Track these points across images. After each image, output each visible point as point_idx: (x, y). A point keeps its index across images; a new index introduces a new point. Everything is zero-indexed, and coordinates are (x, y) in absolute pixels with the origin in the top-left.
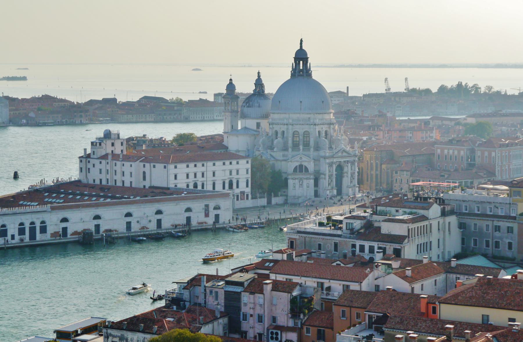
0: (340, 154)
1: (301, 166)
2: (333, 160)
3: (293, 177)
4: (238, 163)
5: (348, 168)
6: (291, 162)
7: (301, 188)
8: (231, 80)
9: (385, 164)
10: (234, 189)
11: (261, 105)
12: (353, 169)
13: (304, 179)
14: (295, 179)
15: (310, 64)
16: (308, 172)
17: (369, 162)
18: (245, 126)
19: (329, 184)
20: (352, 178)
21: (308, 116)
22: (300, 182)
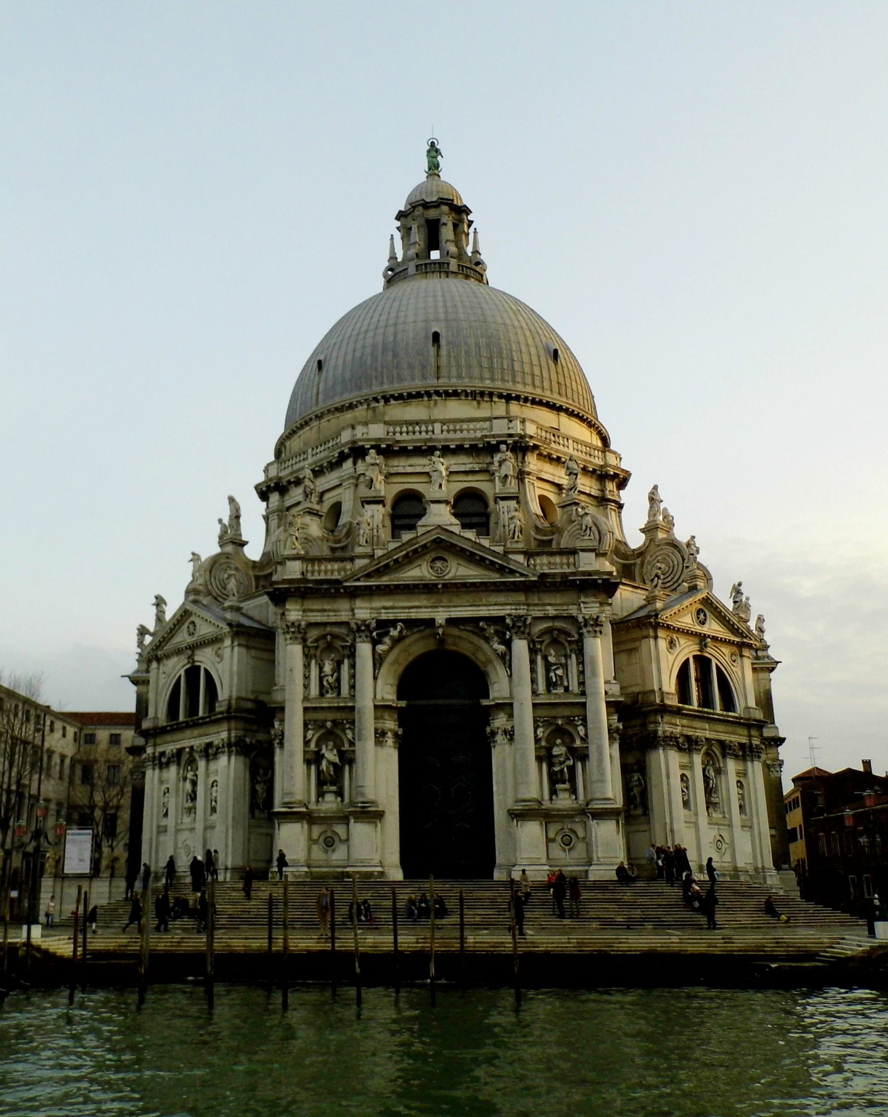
5: (510, 676)
7: (187, 820)
20: (559, 750)
22: (185, 779)
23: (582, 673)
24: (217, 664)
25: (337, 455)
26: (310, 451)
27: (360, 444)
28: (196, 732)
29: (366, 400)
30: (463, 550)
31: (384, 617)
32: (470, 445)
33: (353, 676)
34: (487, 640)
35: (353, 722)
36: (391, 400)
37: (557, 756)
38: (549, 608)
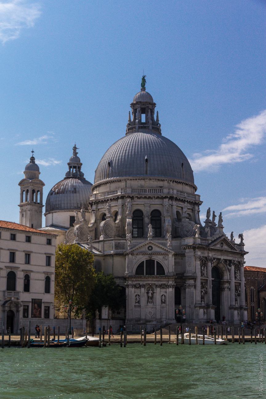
0: (218, 246)
1: (150, 263)
2: (208, 253)
3: (135, 283)
4: (28, 240)
5: (230, 275)
6: (132, 254)
7: (150, 305)
10: (18, 292)
11: (77, 190)
12: (238, 277)
13: (157, 286)
14: (140, 286)
15: (157, 113)
18: (51, 223)
19: (201, 298)
20: (236, 294)
21: (160, 184)
22: (148, 293)
23: (240, 275)
24: (164, 261)
26: (147, 190)
28: (154, 280)
30: (228, 242)
31: (215, 257)
34: (226, 265)
35: (207, 284)
36: (174, 182)
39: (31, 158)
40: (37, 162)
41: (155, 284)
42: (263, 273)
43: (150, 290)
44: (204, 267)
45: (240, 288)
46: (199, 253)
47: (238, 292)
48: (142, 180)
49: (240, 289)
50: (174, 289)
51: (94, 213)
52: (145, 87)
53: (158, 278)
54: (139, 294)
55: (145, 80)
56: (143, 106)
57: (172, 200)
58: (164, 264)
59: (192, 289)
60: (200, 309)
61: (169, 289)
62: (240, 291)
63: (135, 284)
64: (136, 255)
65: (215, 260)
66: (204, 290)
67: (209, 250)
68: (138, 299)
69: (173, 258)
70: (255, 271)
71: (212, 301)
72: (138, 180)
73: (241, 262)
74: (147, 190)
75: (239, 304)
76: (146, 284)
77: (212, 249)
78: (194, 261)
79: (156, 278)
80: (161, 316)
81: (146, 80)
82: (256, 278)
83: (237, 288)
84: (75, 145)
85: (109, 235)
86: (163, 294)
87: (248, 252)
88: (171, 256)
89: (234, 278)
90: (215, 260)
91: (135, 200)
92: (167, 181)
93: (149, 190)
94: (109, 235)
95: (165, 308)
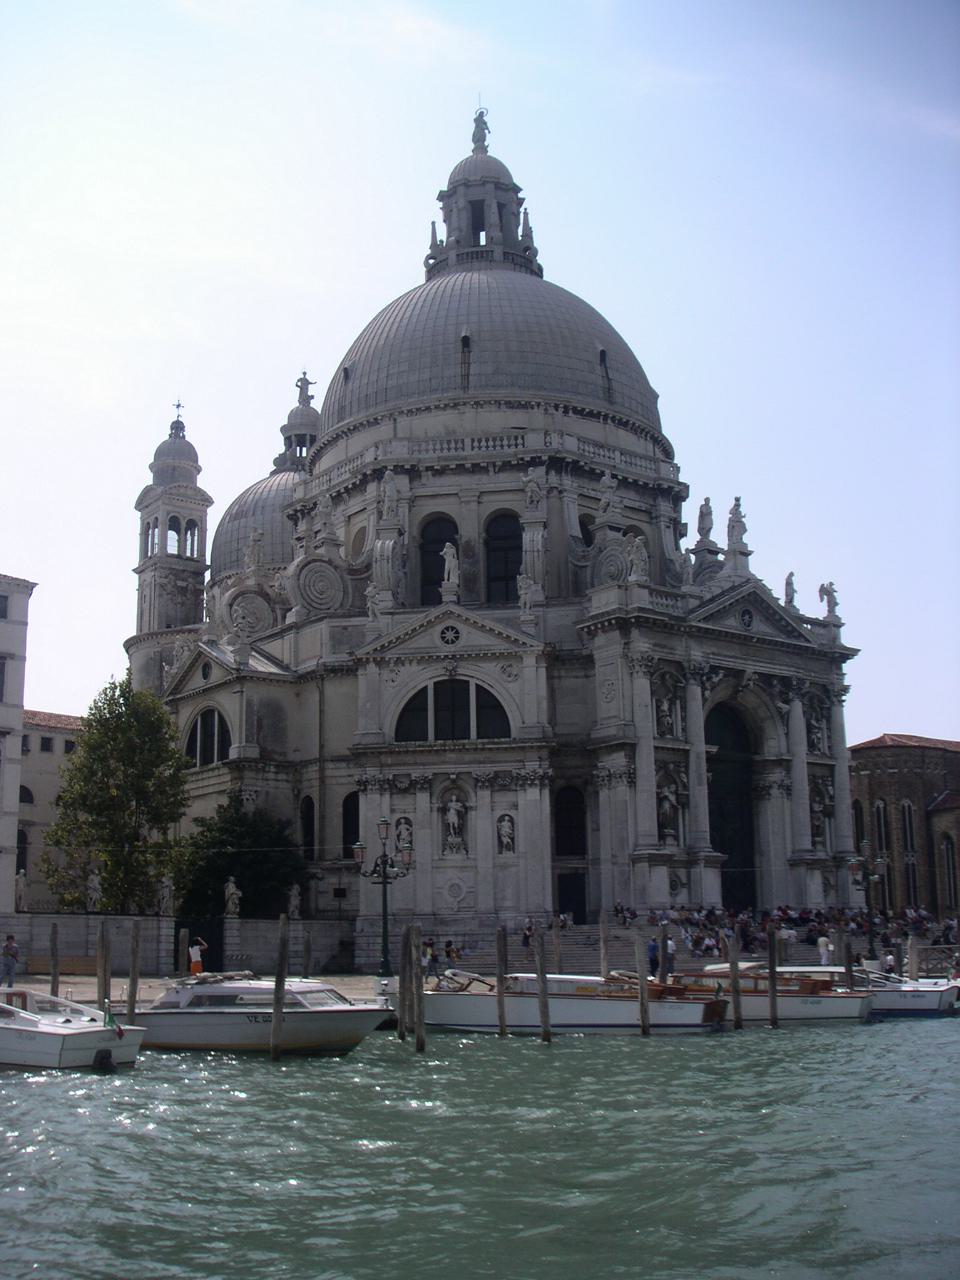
0: (732, 624)
1: (451, 692)
2: (688, 647)
3: (396, 771)
5: (787, 734)
6: (380, 663)
7: (454, 858)
8: (178, 427)
9: (951, 809)
12: (824, 746)
13: (477, 780)
14: (412, 787)
16: (507, 733)
17: (866, 805)
19: (661, 826)
21: (518, 418)
22: (444, 810)
23: (829, 737)
25: (529, 459)
26: (468, 442)
27: (565, 455)
28: (467, 757)
29: (547, 404)
32: (644, 483)
33: (684, 719)
34: (771, 695)
35: (687, 767)
36: (571, 412)
37: (817, 812)
38: (813, 674)
39: (173, 423)
40: (190, 435)
41: (470, 773)
42: (940, 753)
43: (451, 801)
44: (672, 703)
45: (833, 785)
46: (641, 644)
47: (827, 801)
48: (449, 411)
49: (830, 788)
50: (546, 792)
51: (301, 547)
52: (486, 143)
53: (483, 749)
54: (410, 816)
55: (485, 123)
56: (476, 194)
57: (559, 472)
58: (506, 693)
59: (622, 788)
60: (650, 866)
61: (525, 790)
62: (832, 798)
63: (391, 777)
64: (396, 663)
65: (717, 675)
66: (676, 793)
67: (690, 635)
68: (405, 834)
69: (543, 672)
70: (915, 747)
71: (708, 836)
72: (434, 412)
73: (830, 687)
74: (468, 442)
75: (829, 850)
76: (435, 774)
77: (700, 629)
78: (627, 678)
79: (476, 749)
80: (495, 899)
81: (488, 125)
82: (919, 771)
83: (821, 787)
84: (305, 374)
85: (322, 607)
86: (503, 812)
87: (859, 650)
88: (534, 660)
89: (802, 748)
90: (717, 675)
91: (424, 480)
92: (542, 408)
93: (473, 441)
94: (322, 607)
95: (514, 869)
